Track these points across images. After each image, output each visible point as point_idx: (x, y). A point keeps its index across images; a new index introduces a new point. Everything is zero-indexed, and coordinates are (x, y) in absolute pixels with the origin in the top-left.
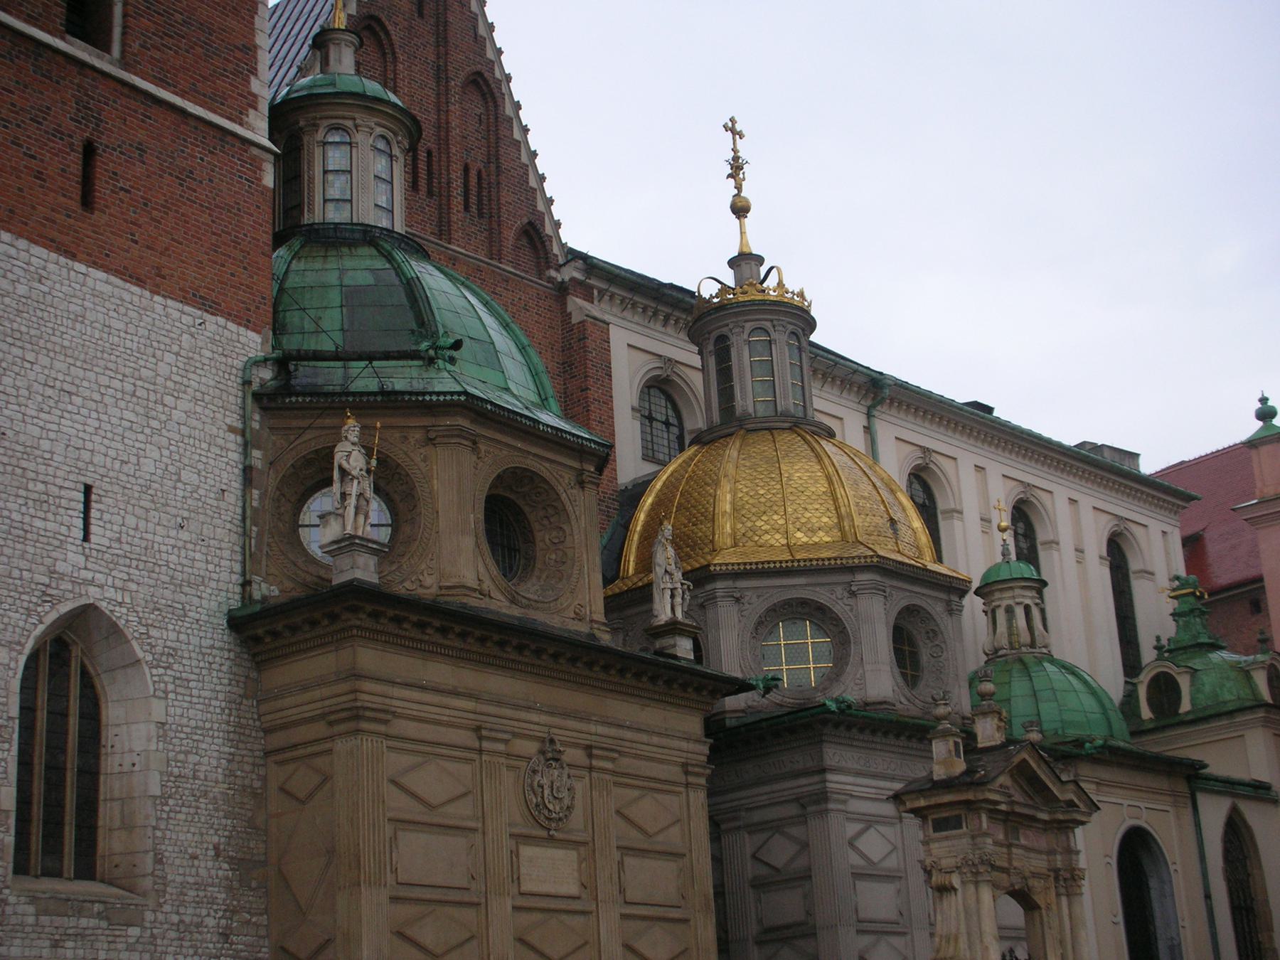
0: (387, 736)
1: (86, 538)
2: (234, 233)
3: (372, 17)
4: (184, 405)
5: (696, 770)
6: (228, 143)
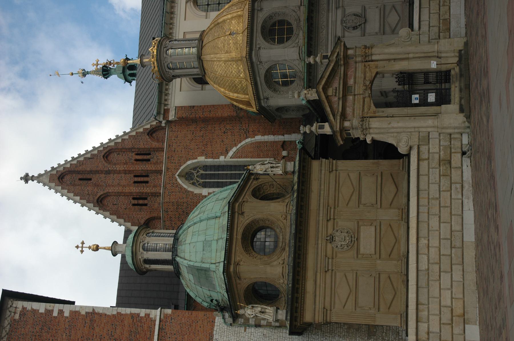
0: (331, 310)
2: (188, 326)
3: (97, 201)
5: (331, 167)
6: (162, 327)
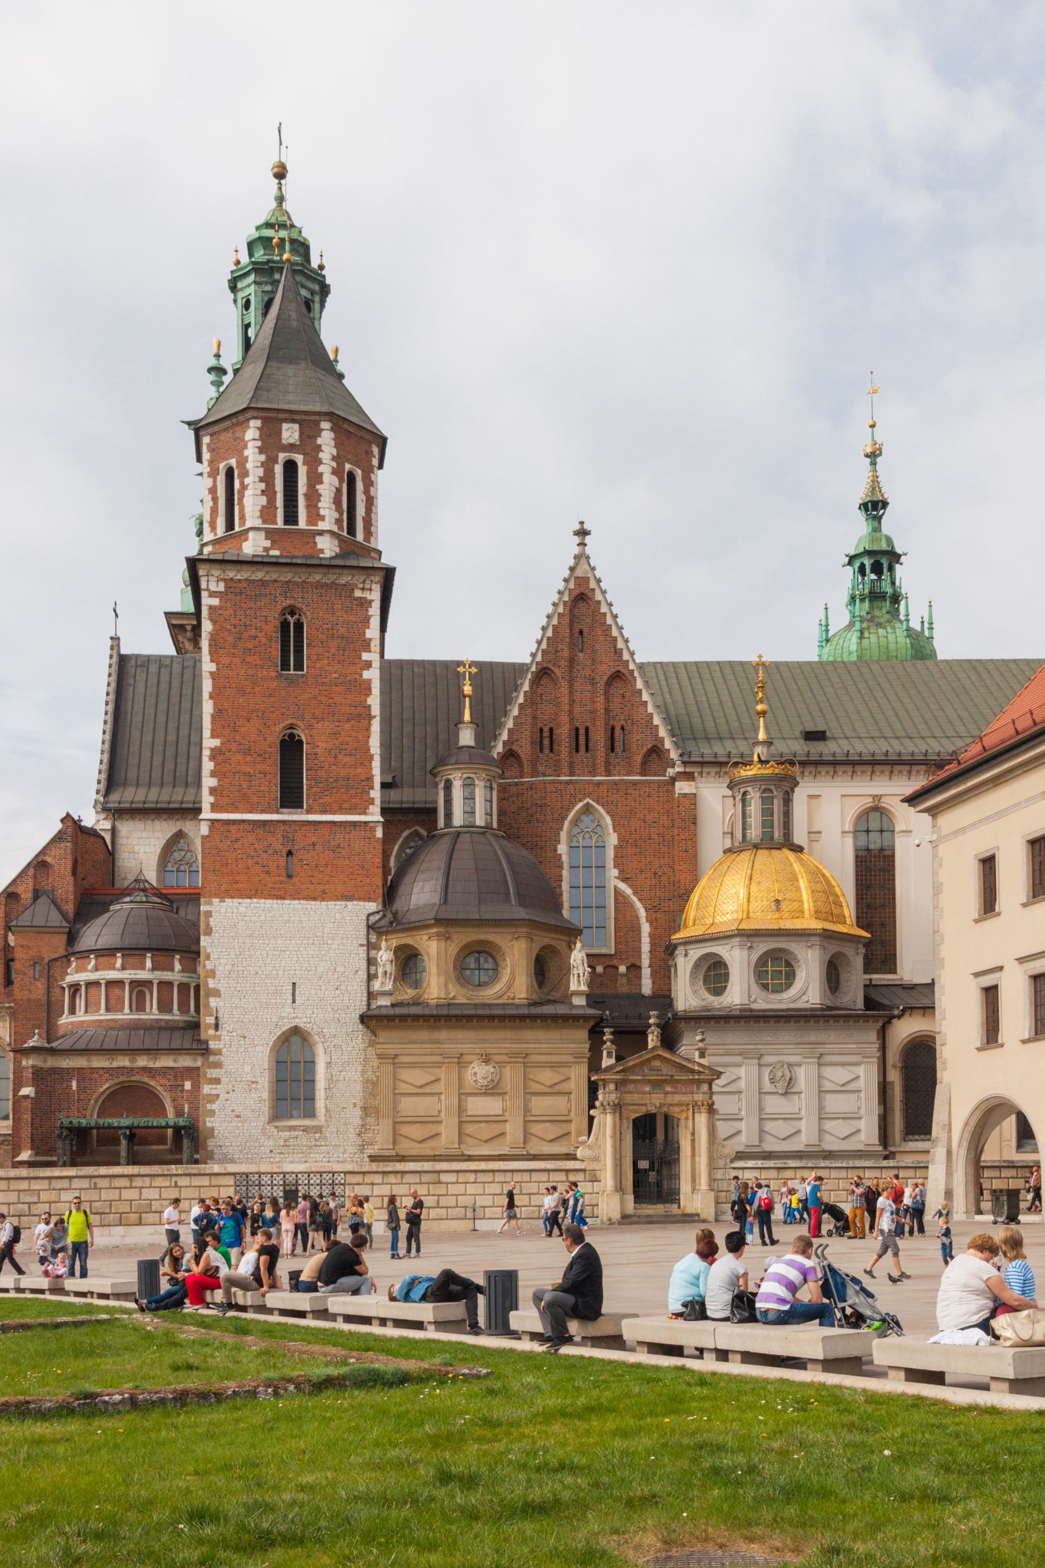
1: (294, 1002)
3: (545, 668)
4: (336, 942)
